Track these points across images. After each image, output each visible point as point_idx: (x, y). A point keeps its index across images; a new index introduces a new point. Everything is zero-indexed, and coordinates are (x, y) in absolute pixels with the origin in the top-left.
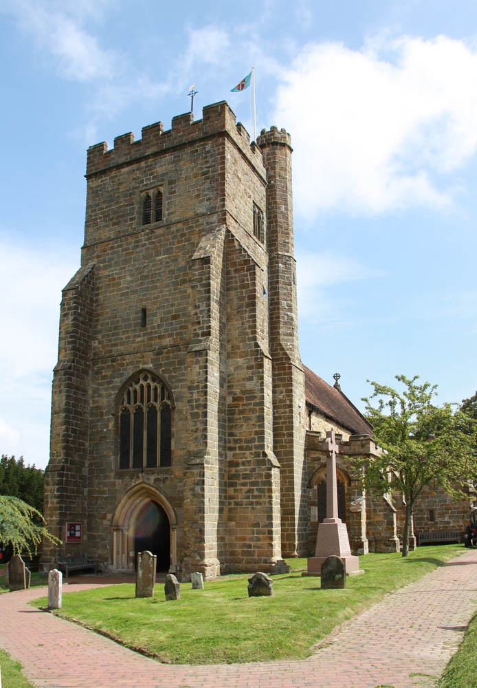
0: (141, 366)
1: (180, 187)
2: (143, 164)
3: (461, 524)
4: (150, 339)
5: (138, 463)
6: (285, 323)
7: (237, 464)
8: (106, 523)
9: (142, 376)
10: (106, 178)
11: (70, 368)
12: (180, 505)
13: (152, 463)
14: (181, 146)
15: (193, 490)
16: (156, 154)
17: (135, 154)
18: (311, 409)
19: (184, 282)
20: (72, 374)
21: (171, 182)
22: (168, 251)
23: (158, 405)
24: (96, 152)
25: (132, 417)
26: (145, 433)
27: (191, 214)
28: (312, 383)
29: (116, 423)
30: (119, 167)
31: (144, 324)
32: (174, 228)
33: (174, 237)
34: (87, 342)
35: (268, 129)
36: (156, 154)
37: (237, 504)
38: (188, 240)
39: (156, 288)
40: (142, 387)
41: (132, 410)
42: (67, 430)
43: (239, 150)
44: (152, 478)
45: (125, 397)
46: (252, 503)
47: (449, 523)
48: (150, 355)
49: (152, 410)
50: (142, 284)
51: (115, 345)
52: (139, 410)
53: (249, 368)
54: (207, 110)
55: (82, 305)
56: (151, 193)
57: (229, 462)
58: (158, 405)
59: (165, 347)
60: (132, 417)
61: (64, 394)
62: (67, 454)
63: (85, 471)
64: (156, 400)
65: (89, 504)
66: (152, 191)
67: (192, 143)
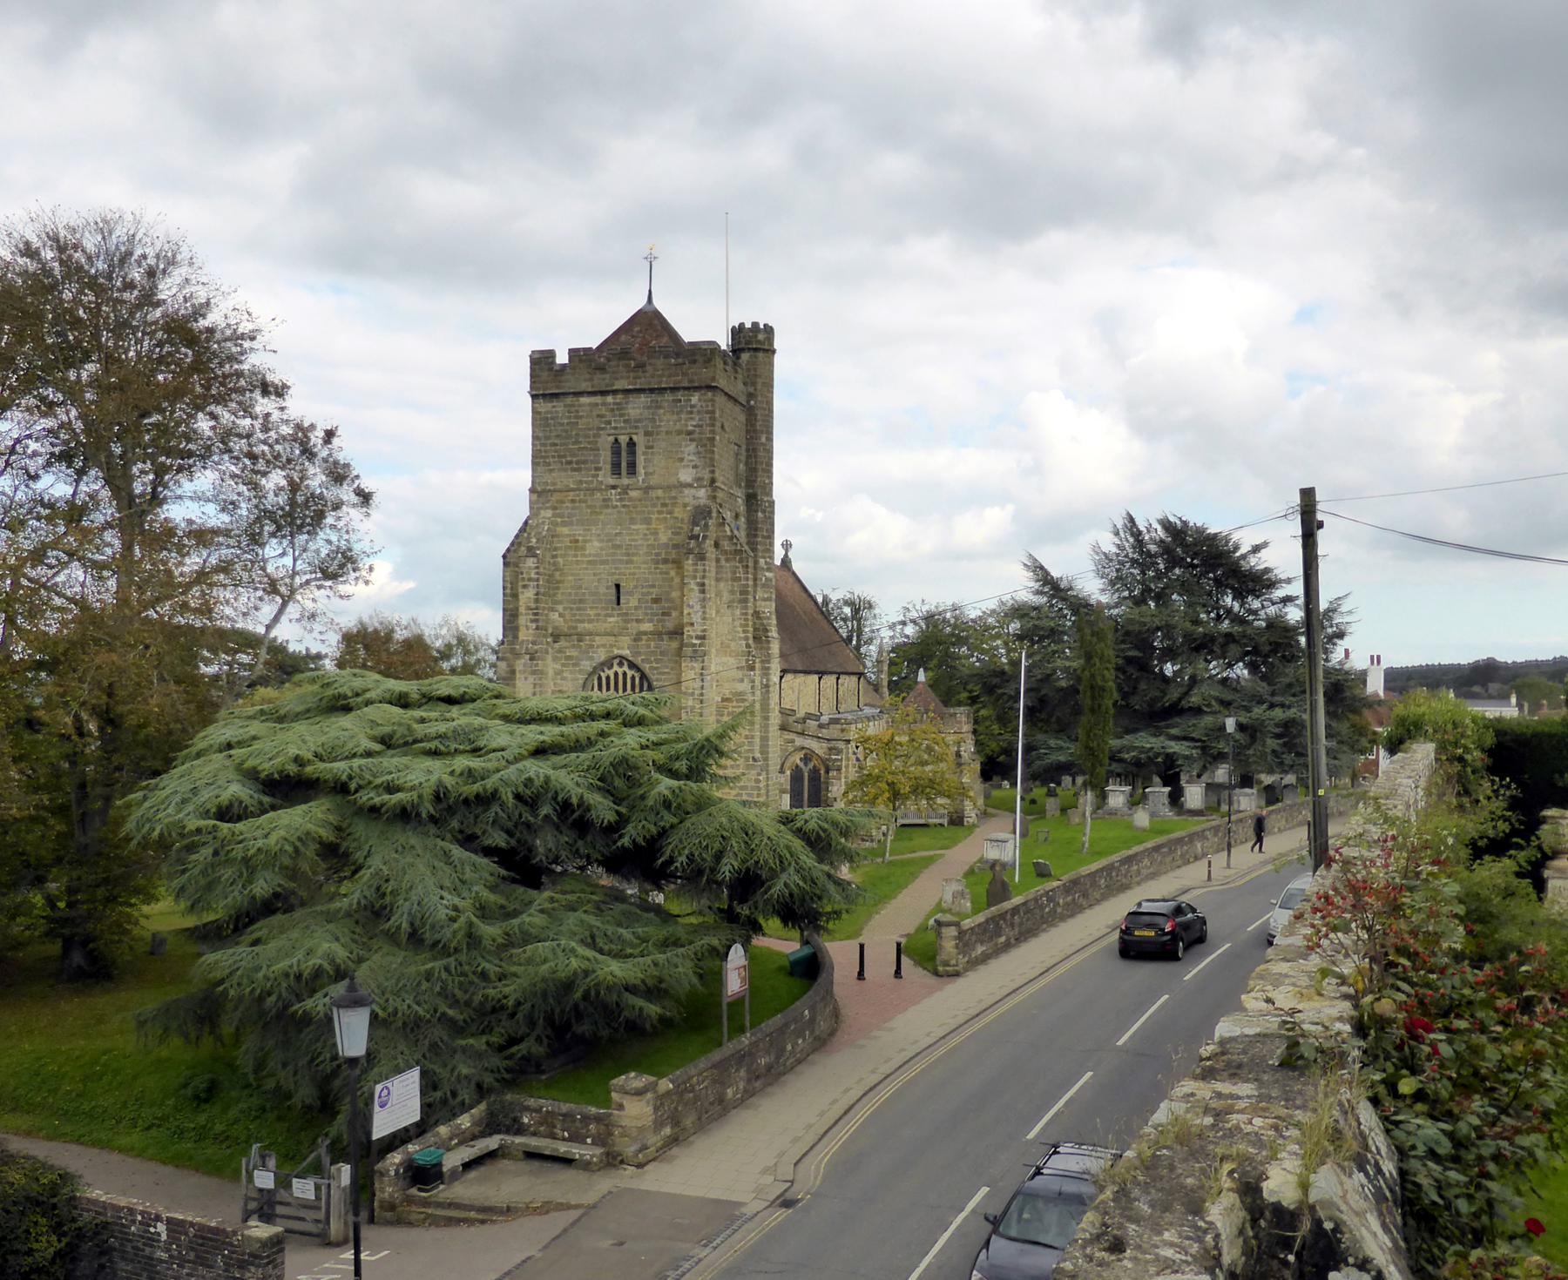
0: (616, 652)
2: (610, 399)
4: (627, 621)
22: (647, 521)
32: (653, 494)
33: (654, 505)
38: (670, 513)
39: (631, 562)
40: (616, 674)
48: (626, 640)
50: (613, 554)
51: (582, 621)
59: (645, 633)
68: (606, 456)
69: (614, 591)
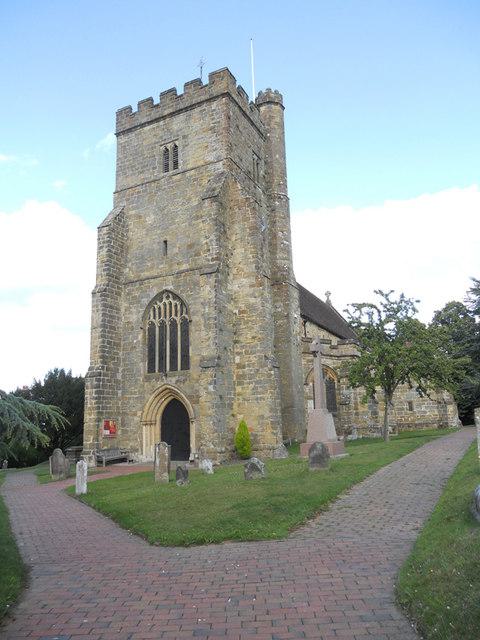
1: (193, 140)
2: (162, 123)
3: (436, 413)
5: (162, 368)
7: (244, 367)
8: (137, 419)
9: (164, 296)
10: (132, 135)
11: (105, 290)
12: (197, 402)
13: (174, 367)
14: (192, 107)
15: (206, 388)
16: (172, 115)
17: (155, 114)
18: (306, 318)
19: (197, 218)
20: (107, 296)
21: (184, 137)
23: (178, 320)
24: (124, 113)
25: (157, 329)
26: (168, 342)
27: (202, 163)
28: (305, 295)
29: (144, 336)
30: (142, 125)
31: (166, 253)
32: (188, 174)
34: (119, 269)
35: (264, 91)
36: (172, 115)
37: (244, 399)
40: (165, 304)
41: (157, 325)
42: (103, 342)
44: (174, 380)
45: (152, 313)
46: (257, 399)
47: (425, 412)
49: (173, 324)
51: (142, 271)
52: (163, 324)
53: (252, 286)
54: (212, 76)
55: (114, 237)
56: (169, 146)
57: (238, 364)
58: (178, 320)
60: (157, 329)
61: (101, 312)
62: (104, 362)
63: (119, 376)
64: (176, 315)
65: (123, 403)
66: (169, 145)
67: (200, 104)
68: (159, 159)
69: (163, 245)
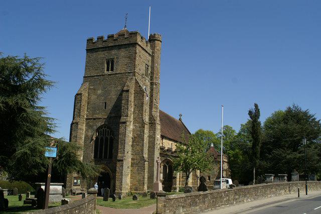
5: (101, 157)
6: (155, 107)
17: (104, 45)
18: (163, 137)
23: (109, 137)
26: (104, 146)
43: (142, 47)
49: (107, 139)
58: (109, 137)
